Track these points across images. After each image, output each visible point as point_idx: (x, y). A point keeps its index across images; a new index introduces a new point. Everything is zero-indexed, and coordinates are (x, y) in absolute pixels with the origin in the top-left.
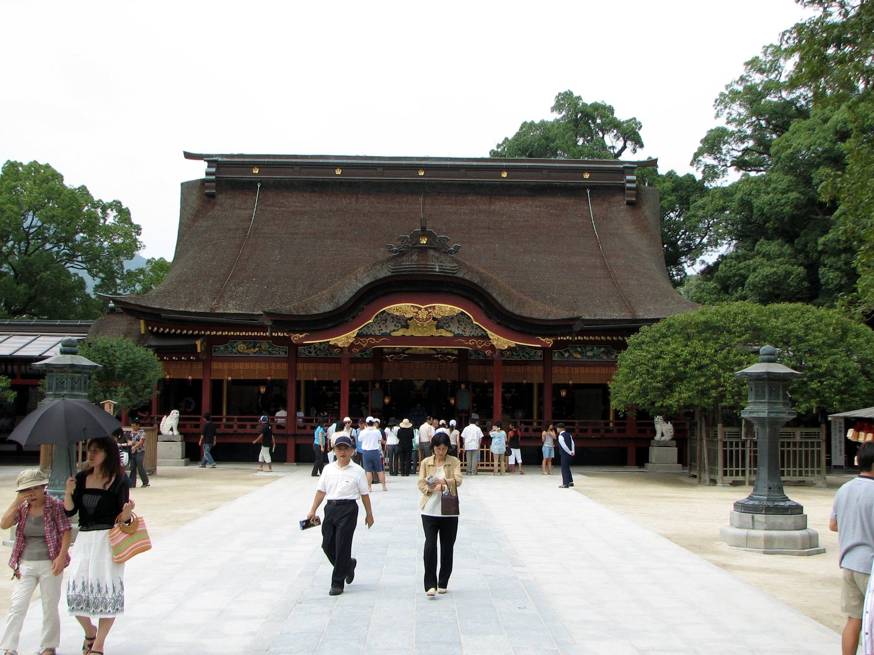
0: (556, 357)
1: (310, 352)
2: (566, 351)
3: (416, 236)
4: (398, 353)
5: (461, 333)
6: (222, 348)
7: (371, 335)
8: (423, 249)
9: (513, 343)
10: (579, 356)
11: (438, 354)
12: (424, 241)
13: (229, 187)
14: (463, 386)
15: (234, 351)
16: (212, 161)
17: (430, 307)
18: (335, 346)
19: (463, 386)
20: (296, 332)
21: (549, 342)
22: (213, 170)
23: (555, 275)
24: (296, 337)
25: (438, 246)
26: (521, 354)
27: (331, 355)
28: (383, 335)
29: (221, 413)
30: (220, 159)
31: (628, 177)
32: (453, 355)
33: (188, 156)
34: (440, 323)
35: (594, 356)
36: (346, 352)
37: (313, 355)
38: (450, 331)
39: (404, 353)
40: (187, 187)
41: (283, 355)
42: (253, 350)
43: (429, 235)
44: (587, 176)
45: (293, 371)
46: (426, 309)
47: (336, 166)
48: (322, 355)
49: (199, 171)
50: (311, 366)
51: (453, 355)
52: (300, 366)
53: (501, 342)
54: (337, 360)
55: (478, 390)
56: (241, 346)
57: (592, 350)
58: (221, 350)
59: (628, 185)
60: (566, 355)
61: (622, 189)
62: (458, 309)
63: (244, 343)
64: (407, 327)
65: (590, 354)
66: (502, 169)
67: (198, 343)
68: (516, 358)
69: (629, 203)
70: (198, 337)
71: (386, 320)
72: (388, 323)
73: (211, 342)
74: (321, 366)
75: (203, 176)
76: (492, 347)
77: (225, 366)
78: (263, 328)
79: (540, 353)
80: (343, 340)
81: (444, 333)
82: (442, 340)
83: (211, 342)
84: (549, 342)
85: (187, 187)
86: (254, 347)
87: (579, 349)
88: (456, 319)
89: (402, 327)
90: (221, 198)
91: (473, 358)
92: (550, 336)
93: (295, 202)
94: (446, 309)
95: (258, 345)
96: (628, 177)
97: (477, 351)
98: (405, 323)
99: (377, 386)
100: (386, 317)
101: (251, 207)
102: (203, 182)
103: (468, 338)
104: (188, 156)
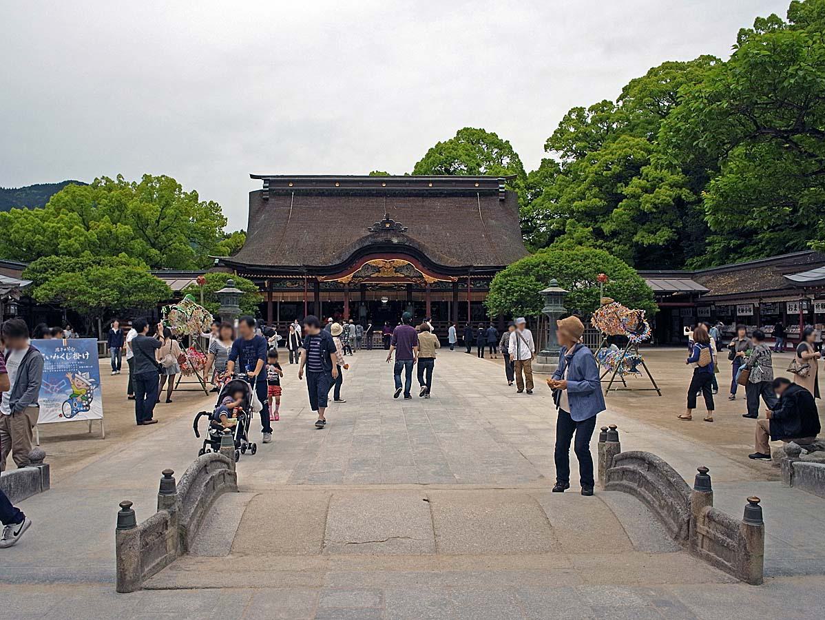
3: (384, 223)
7: (360, 277)
8: (388, 230)
9: (436, 280)
13: (276, 194)
14: (409, 303)
16: (266, 179)
18: (342, 283)
19: (409, 303)
20: (320, 275)
21: (456, 279)
22: (268, 185)
24: (320, 278)
25: (394, 229)
27: (337, 288)
28: (367, 276)
29: (277, 320)
30: (270, 178)
31: (500, 186)
32: (404, 287)
33: (252, 176)
35: (481, 286)
36: (347, 286)
40: (252, 194)
41: (311, 288)
43: (391, 222)
45: (317, 296)
47: (336, 182)
49: (259, 185)
50: (327, 294)
52: (321, 294)
54: (342, 290)
55: (418, 306)
56: (289, 284)
57: (479, 283)
59: (500, 190)
61: (496, 193)
64: (379, 272)
67: (266, 282)
68: (438, 288)
69: (501, 200)
70: (265, 279)
73: (272, 281)
74: (332, 294)
75: (262, 188)
76: (425, 282)
77: (280, 294)
79: (451, 285)
80: (345, 279)
82: (398, 279)
83: (272, 281)
84: (456, 279)
85: (252, 194)
86: (296, 284)
89: (377, 272)
90: (272, 200)
92: (456, 276)
93: (314, 202)
96: (500, 186)
98: (378, 270)
99: (363, 304)
100: (367, 267)
103: (412, 278)
104: (252, 176)
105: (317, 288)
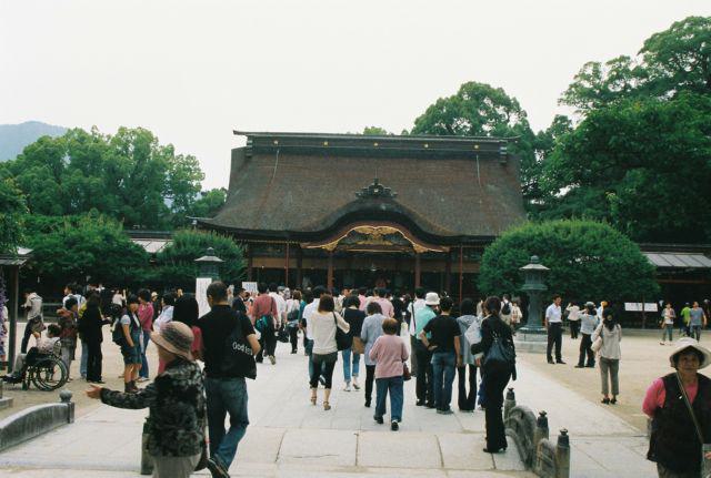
3: (372, 188)
8: (376, 196)
12: (376, 191)
16: (250, 136)
23: (446, 207)
24: (303, 245)
25: (384, 195)
27: (322, 254)
33: (235, 133)
34: (385, 237)
44: (476, 147)
47: (324, 140)
49: (242, 142)
53: (420, 248)
56: (270, 249)
61: (497, 155)
62: (395, 230)
66: (424, 142)
69: (502, 164)
78: (285, 239)
80: (329, 246)
81: (387, 243)
82: (386, 247)
85: (235, 152)
90: (254, 159)
94: (390, 229)
97: (407, 254)
98: (365, 237)
100: (354, 234)
101: (275, 165)
102: (244, 149)
104: (235, 133)
105: (301, 254)
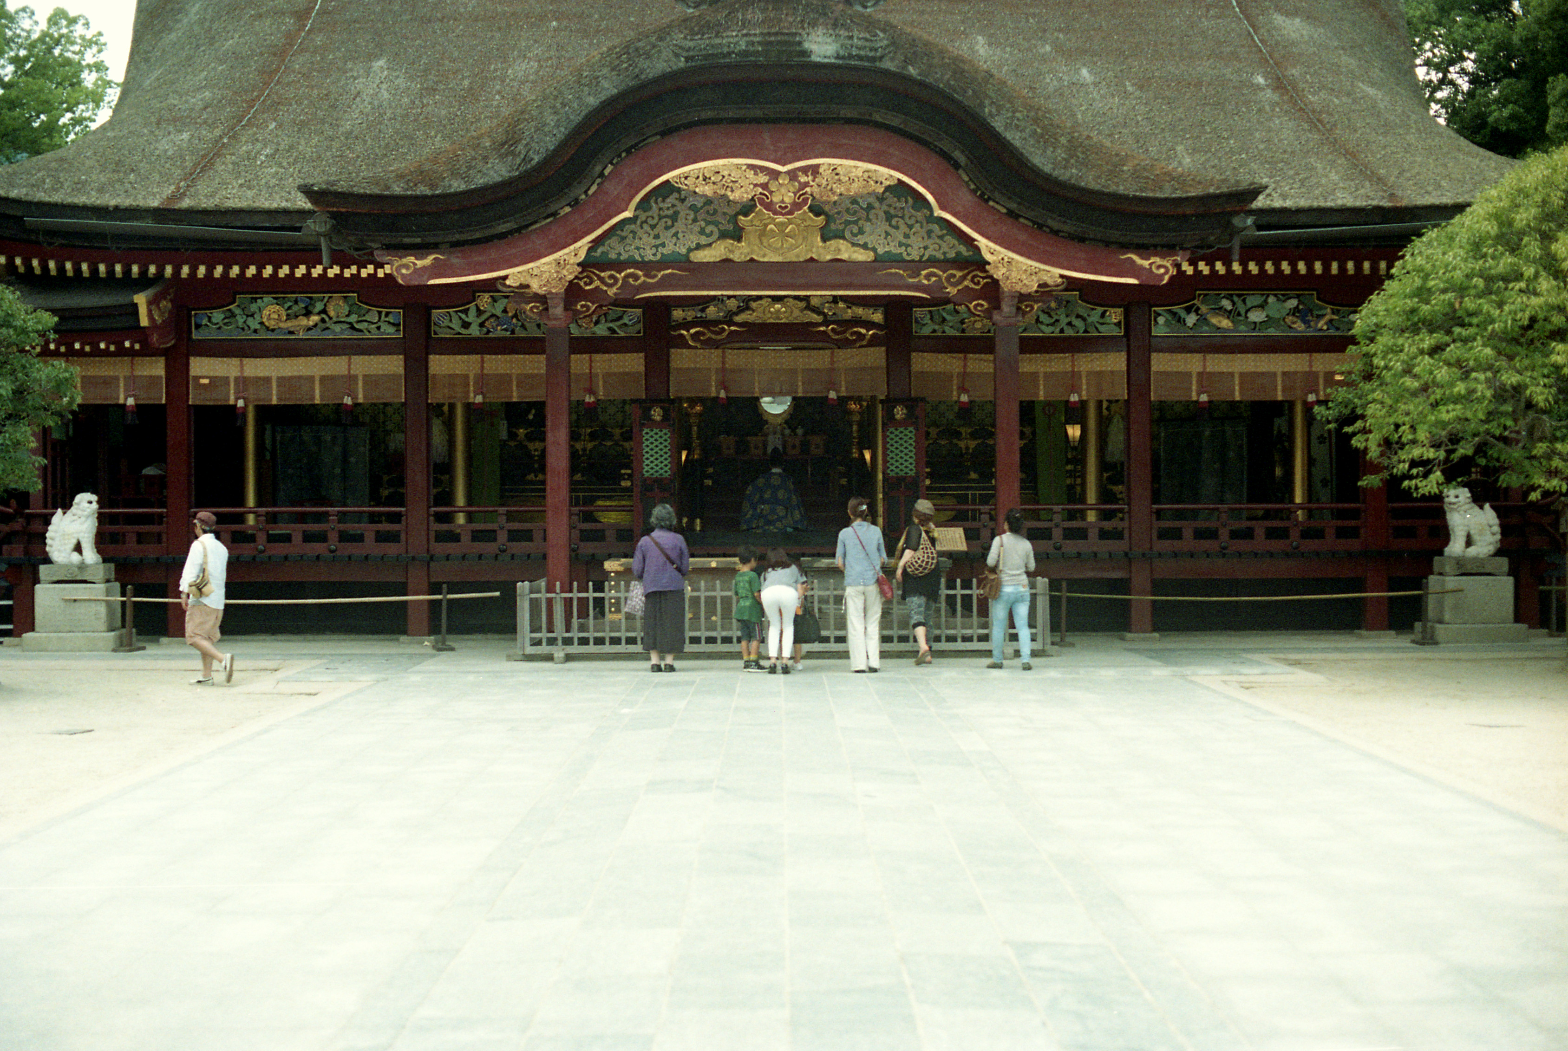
0: (1161, 327)
1: (466, 325)
2: (1188, 310)
4: (716, 323)
5: (893, 248)
6: (218, 316)
10: (1225, 323)
11: (826, 323)
15: (253, 324)
17: (805, 170)
26: (1064, 320)
35: (1270, 321)
37: (474, 331)
38: (865, 246)
39: (731, 323)
41: (389, 331)
42: (304, 322)
46: (793, 175)
48: (499, 332)
51: (869, 325)
57: (1262, 306)
58: (213, 323)
60: (1191, 319)
63: (279, 302)
65: (1256, 316)
68: (1048, 331)
71: (674, 217)
72: (680, 226)
86: (308, 313)
87: (1226, 304)
88: (880, 210)
89: (723, 235)
91: (926, 331)
95: (319, 306)
